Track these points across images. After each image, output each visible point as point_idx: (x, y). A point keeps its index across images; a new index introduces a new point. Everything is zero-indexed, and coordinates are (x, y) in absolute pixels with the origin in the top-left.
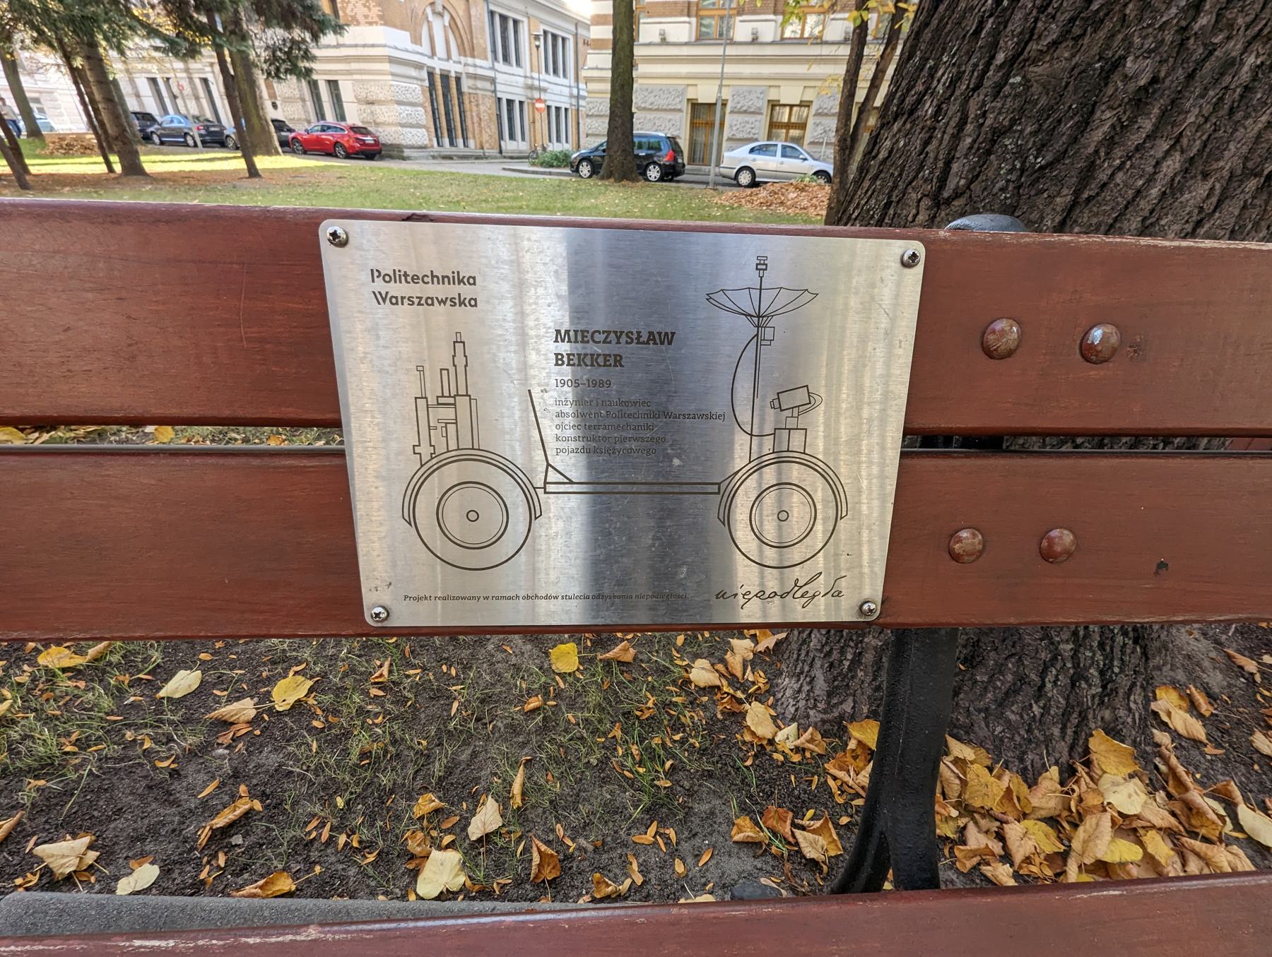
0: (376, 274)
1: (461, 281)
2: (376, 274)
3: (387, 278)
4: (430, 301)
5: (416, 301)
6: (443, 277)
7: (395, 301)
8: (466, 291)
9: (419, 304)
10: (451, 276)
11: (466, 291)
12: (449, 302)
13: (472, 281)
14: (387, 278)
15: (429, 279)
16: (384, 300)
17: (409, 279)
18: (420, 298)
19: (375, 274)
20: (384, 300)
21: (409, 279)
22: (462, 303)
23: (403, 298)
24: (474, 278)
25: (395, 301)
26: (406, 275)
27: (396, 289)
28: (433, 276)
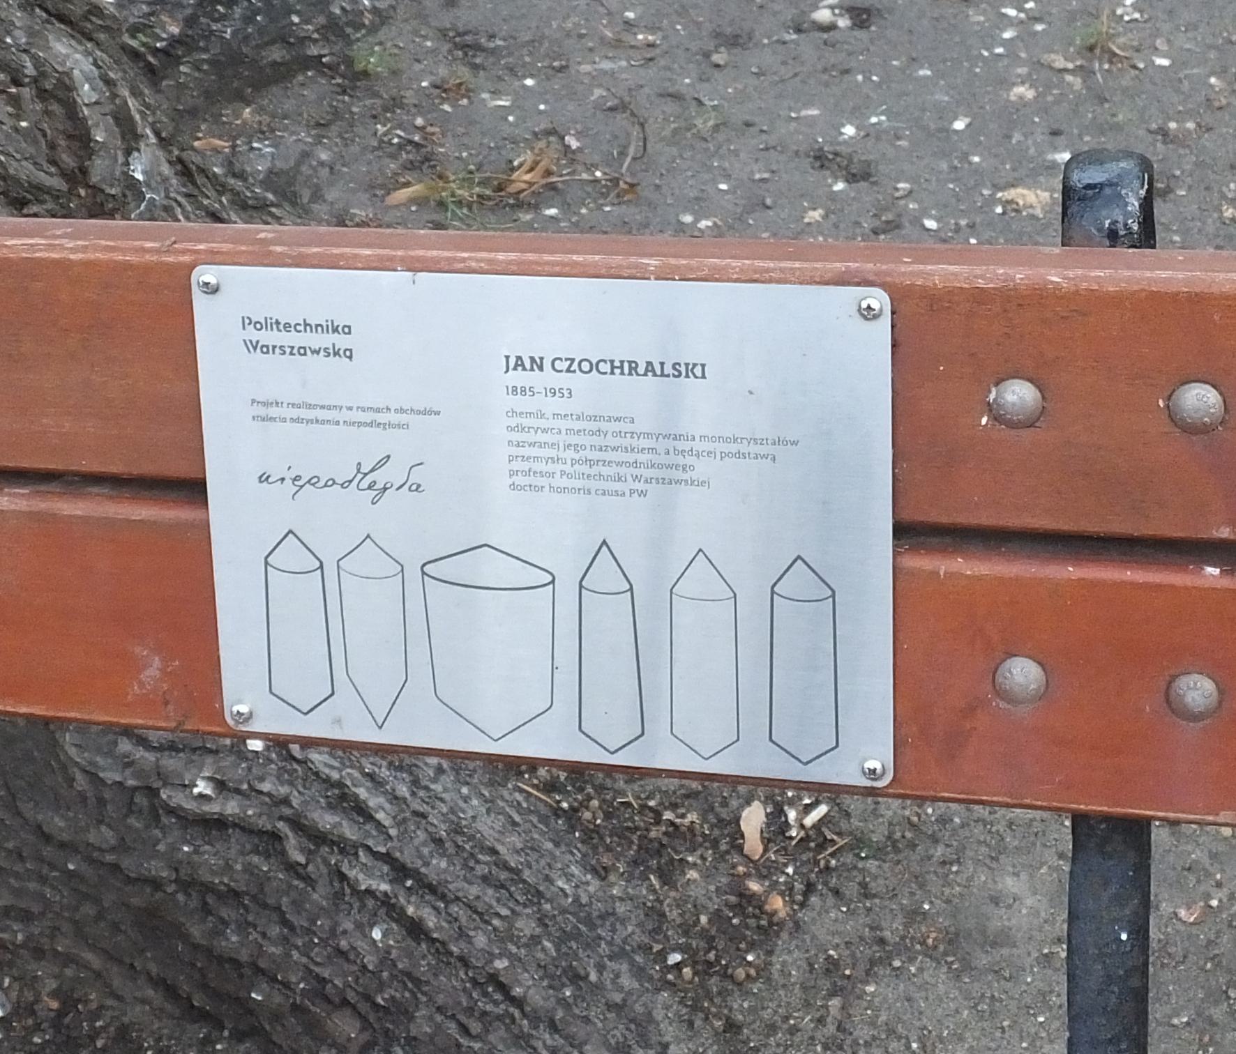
0: (247, 321)
1: (335, 330)
2: (247, 321)
3: (258, 326)
4: (303, 351)
5: (288, 350)
6: (317, 326)
7: (266, 350)
8: (341, 341)
9: (291, 354)
10: (324, 324)
11: (341, 341)
12: (322, 353)
13: (347, 330)
14: (258, 326)
15: (301, 328)
16: (255, 348)
17: (281, 327)
18: (292, 348)
19: (247, 322)
20: (255, 348)
21: (281, 327)
22: (336, 353)
23: (274, 347)
24: (349, 327)
25: (266, 350)
26: (278, 323)
27: (268, 337)
28: (306, 325)
